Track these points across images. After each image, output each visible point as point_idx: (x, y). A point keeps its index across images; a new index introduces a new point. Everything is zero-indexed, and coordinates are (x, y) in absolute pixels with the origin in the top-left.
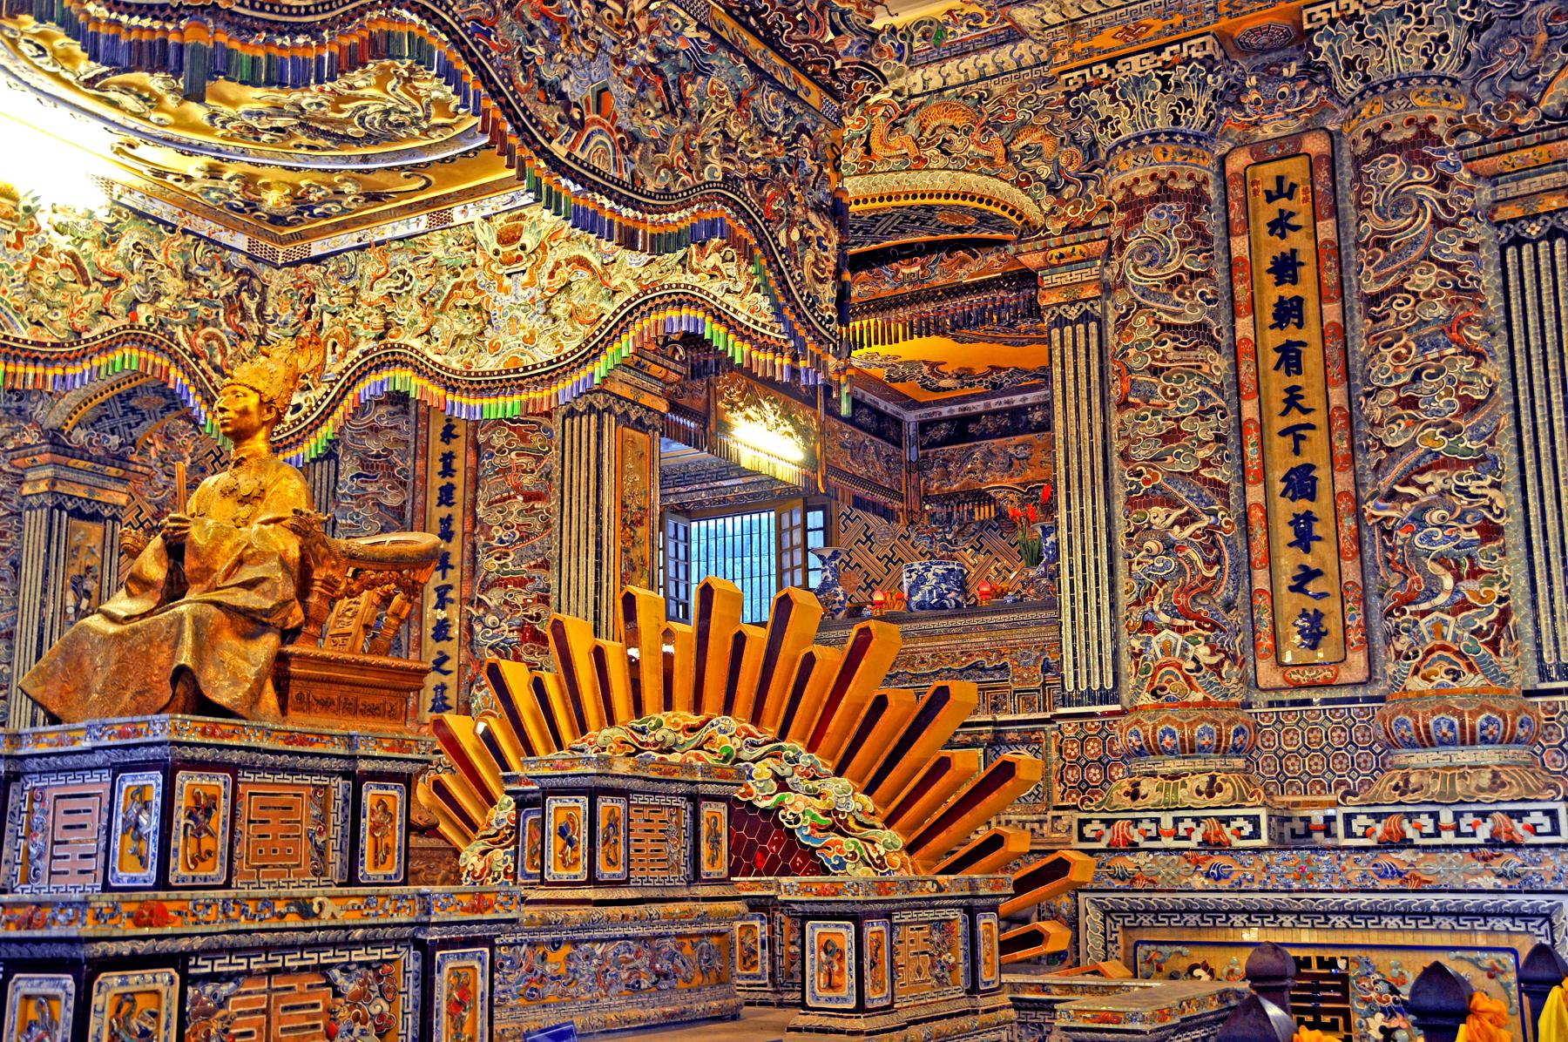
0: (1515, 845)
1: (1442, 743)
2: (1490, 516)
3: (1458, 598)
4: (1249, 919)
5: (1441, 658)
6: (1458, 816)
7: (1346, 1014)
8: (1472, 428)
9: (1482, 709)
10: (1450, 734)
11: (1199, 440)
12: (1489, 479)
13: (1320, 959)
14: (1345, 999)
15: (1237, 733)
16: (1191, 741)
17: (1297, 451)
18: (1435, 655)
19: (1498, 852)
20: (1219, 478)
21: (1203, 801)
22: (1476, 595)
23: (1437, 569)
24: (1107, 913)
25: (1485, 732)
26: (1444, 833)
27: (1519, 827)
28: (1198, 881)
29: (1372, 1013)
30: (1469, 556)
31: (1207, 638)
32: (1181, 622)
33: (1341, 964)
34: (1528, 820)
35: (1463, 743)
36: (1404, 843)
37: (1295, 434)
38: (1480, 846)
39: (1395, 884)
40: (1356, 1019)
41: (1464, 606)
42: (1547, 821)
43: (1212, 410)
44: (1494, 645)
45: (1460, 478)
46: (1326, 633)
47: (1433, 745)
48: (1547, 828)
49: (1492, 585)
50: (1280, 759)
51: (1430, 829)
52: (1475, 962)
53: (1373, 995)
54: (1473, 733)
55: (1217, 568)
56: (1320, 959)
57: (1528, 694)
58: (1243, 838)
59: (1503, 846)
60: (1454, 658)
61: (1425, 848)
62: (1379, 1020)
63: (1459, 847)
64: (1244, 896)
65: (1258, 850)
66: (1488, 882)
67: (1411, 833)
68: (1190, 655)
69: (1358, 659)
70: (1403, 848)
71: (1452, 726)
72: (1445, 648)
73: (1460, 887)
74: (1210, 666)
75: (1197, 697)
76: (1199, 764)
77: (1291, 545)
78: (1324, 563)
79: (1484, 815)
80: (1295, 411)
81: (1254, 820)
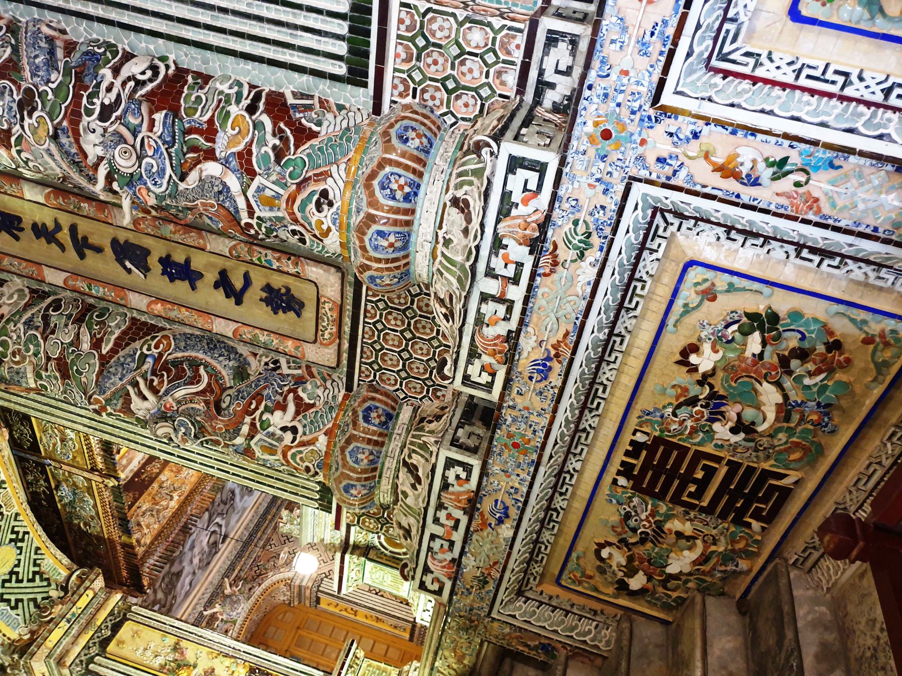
0: (544, 226)
1: (405, 247)
2: (149, 87)
3: (234, 163)
4: (561, 494)
5: (302, 208)
6: (490, 273)
7: (699, 455)
8: (34, 75)
9: (368, 186)
10: (392, 239)
11: (71, 344)
12: (106, 73)
13: (627, 453)
14: (684, 450)
15: (366, 419)
16: (364, 471)
17: (99, 250)
18: (299, 215)
19: (549, 246)
20: (117, 333)
21: (422, 489)
22: (232, 141)
23: (193, 177)
24: (520, 593)
25: (399, 195)
26: (509, 296)
27: (522, 210)
28: (506, 531)
29: (710, 433)
30: (190, 131)
31: (267, 409)
32: (245, 429)
33: (640, 438)
34: (516, 197)
35: (409, 223)
36: (512, 338)
37: (82, 245)
38: (536, 265)
39: (558, 368)
40: (709, 449)
41: (245, 157)
42: (522, 174)
43: (46, 318)
44: (304, 135)
45: (89, 113)
46: (288, 290)
47: (406, 256)
48: (533, 177)
49: (228, 113)
50: (409, 376)
51: (502, 309)
52: (687, 310)
53: (689, 423)
54: (397, 211)
55: (202, 370)
56: (627, 453)
57: (377, 109)
58: (468, 479)
59: (542, 238)
60: (304, 195)
61: (522, 322)
62: (721, 430)
63: (530, 288)
64: (532, 501)
65: (484, 473)
66: (587, 272)
67: (502, 329)
68: (279, 432)
69: (314, 271)
70: (516, 345)
71: (381, 234)
72: (291, 199)
73: (584, 304)
74: (297, 413)
75: (323, 440)
76: (388, 474)
77: (193, 288)
78: (212, 265)
79: (498, 244)
80: (59, 236)
81: (450, 463)
